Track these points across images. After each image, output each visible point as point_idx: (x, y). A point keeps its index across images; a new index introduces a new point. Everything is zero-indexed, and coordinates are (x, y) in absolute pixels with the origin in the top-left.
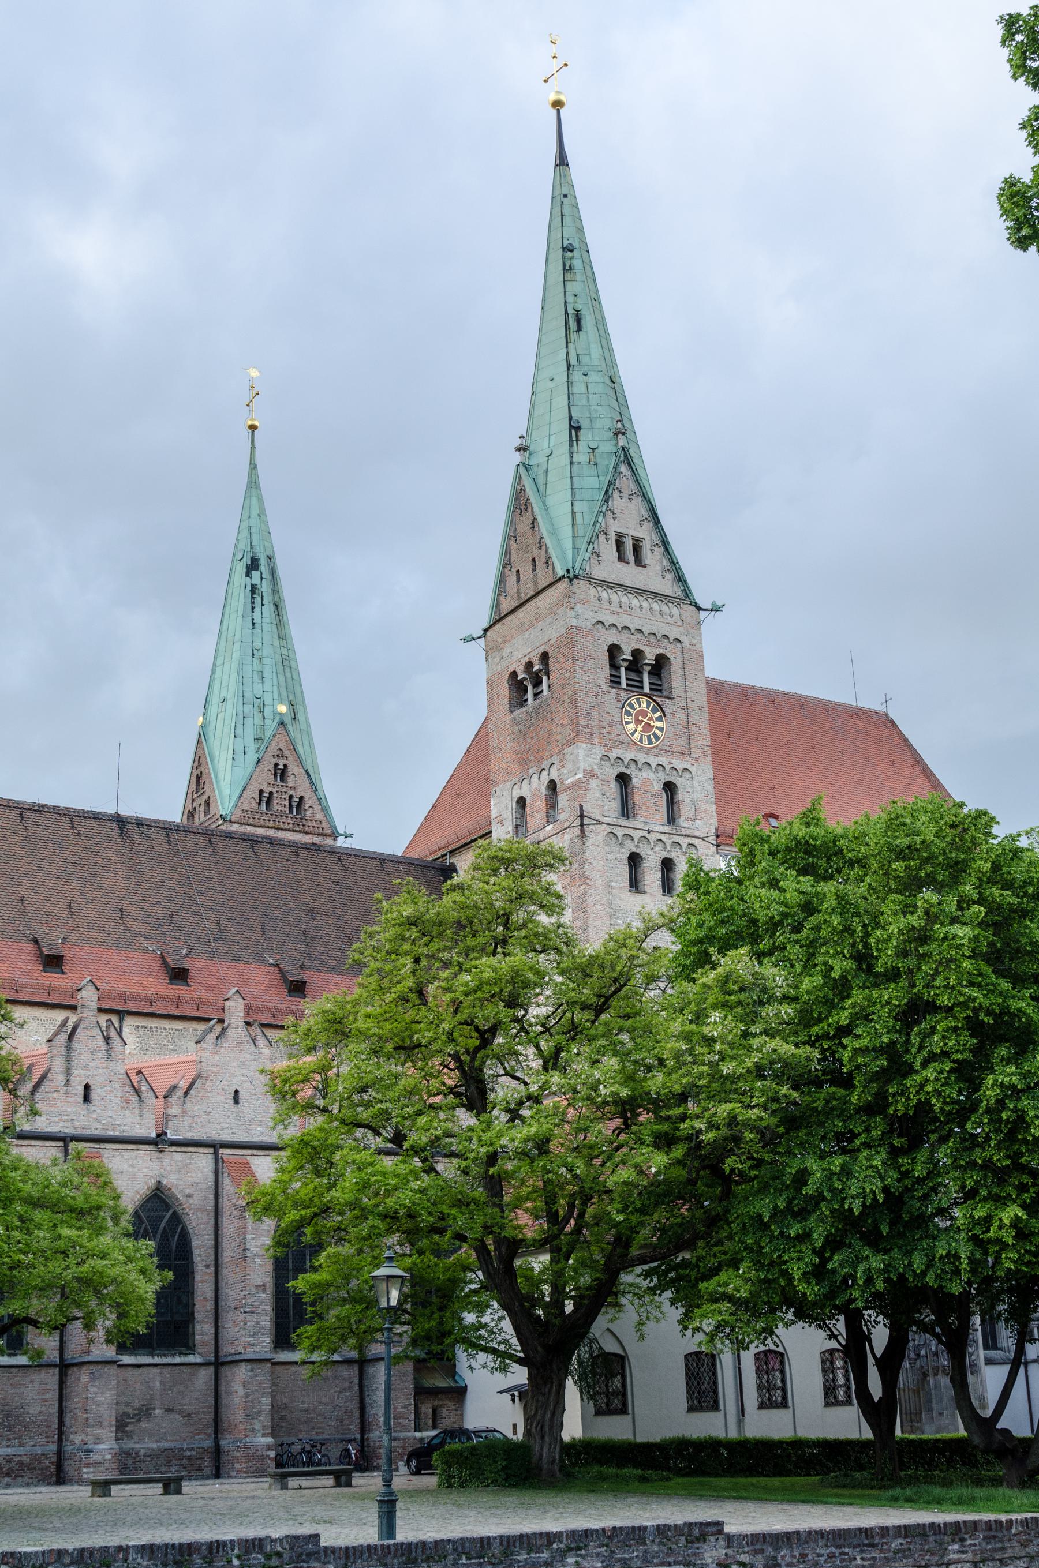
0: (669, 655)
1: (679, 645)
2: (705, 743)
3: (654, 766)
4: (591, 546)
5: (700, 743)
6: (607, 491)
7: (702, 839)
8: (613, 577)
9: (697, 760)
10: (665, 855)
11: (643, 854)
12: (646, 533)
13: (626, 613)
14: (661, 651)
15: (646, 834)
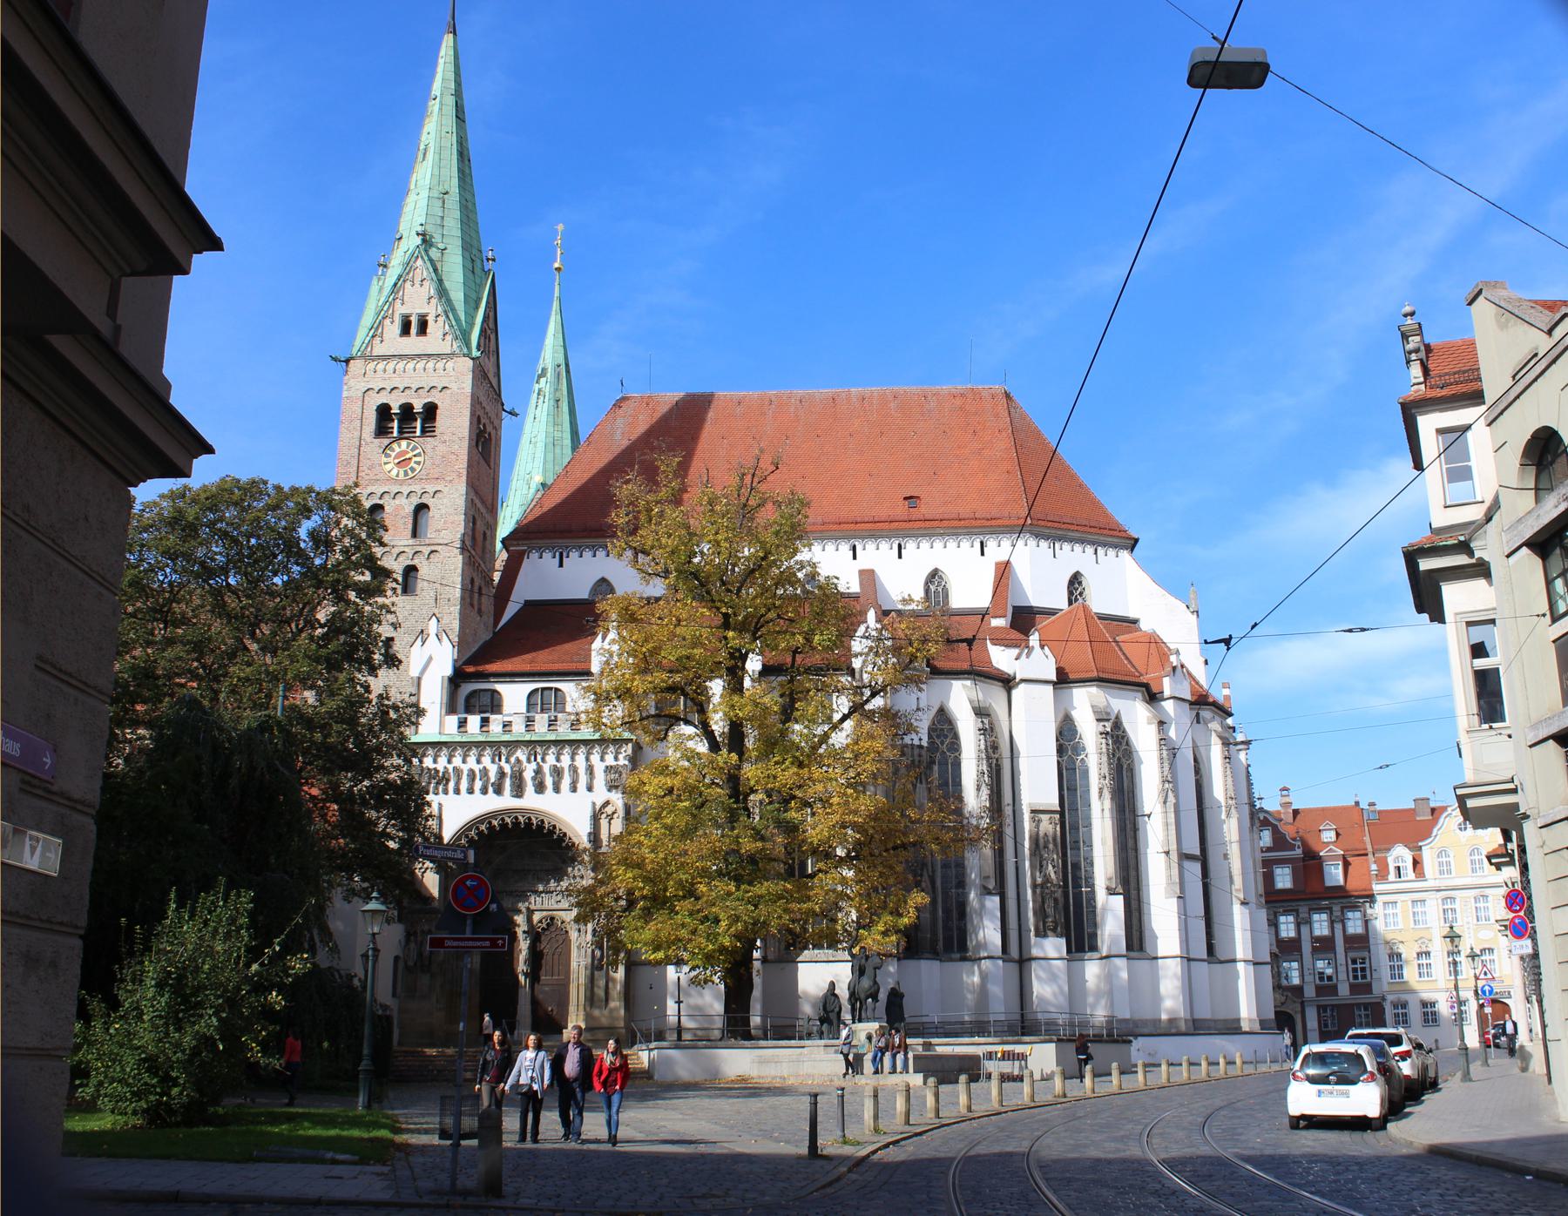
1: (448, 392)
2: (461, 466)
4: (373, 330)
6: (395, 285)
9: (451, 481)
10: (409, 563)
12: (432, 309)
13: (400, 377)
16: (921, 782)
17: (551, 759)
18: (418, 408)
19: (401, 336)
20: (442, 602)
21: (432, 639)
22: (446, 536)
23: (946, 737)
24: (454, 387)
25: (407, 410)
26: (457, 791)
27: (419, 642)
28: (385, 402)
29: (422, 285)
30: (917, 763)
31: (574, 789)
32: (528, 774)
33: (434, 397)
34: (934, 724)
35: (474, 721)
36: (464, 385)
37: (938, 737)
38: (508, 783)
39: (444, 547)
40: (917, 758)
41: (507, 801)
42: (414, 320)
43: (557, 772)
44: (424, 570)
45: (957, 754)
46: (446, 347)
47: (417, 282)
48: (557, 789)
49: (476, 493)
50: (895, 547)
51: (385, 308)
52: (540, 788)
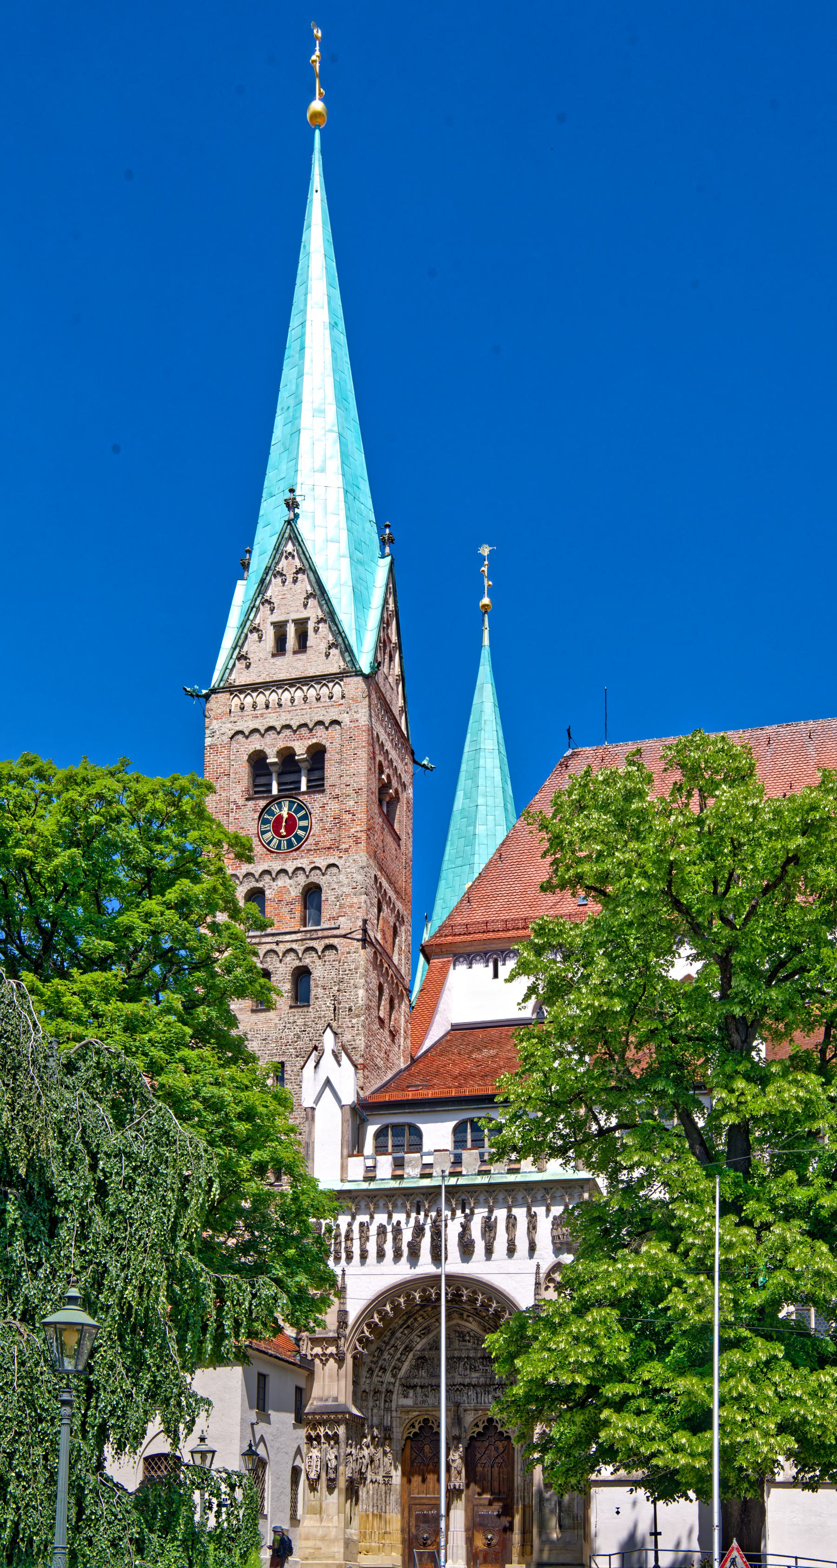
0: (324, 742)
1: (338, 727)
2: (359, 828)
3: (290, 871)
5: (353, 830)
7: (344, 936)
8: (263, 676)
9: (346, 850)
10: (297, 963)
11: (271, 968)
14: (314, 741)
15: (274, 947)
17: (480, 1213)
18: (300, 749)
19: (274, 655)
20: (342, 1014)
21: (328, 1058)
22: (345, 924)
24: (345, 719)
25: (287, 755)
26: (364, 1256)
27: (311, 1063)
28: (258, 748)
29: (295, 581)
31: (511, 1250)
32: (453, 1230)
33: (321, 736)
35: (385, 1166)
36: (356, 716)
38: (426, 1243)
39: (342, 940)
41: (426, 1266)
42: (291, 630)
43: (489, 1227)
44: (319, 971)
46: (336, 663)
47: (290, 579)
48: (489, 1251)
51: (251, 617)
52: (466, 1249)
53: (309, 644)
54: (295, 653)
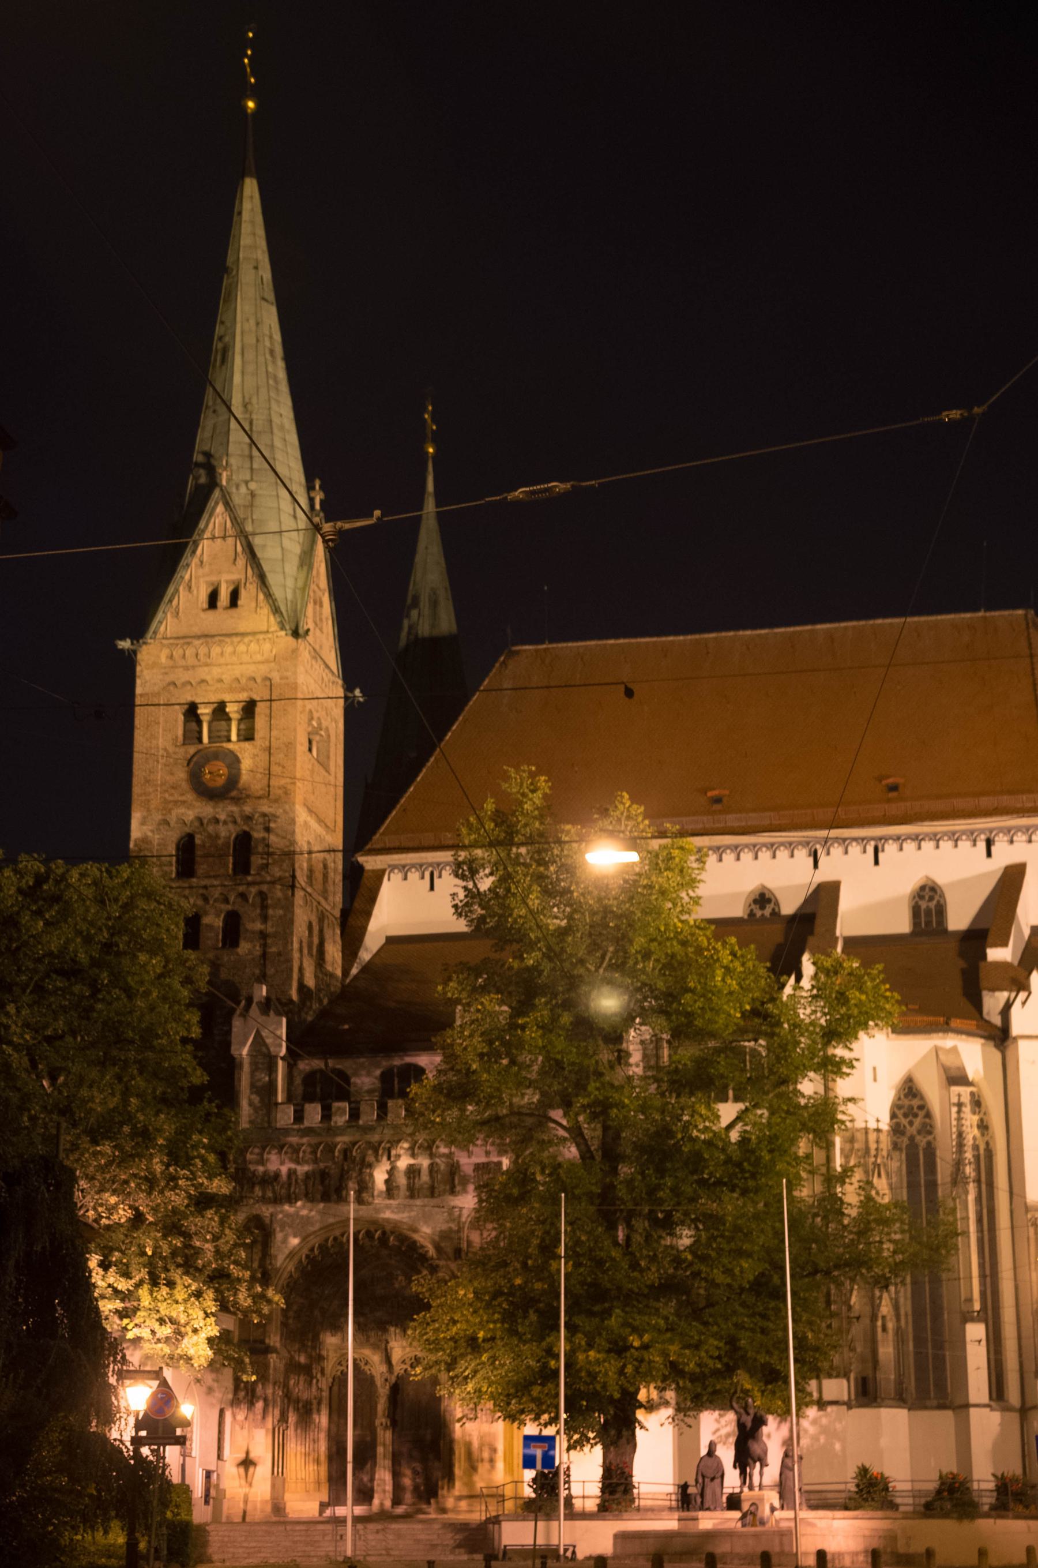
16: (879, 1175)
23: (916, 1116)
30: (873, 1152)
34: (899, 1099)
37: (905, 1116)
40: (873, 1146)
45: (930, 1138)
49: (310, 811)
50: (870, 849)
53: (240, 603)
54: (226, 608)
